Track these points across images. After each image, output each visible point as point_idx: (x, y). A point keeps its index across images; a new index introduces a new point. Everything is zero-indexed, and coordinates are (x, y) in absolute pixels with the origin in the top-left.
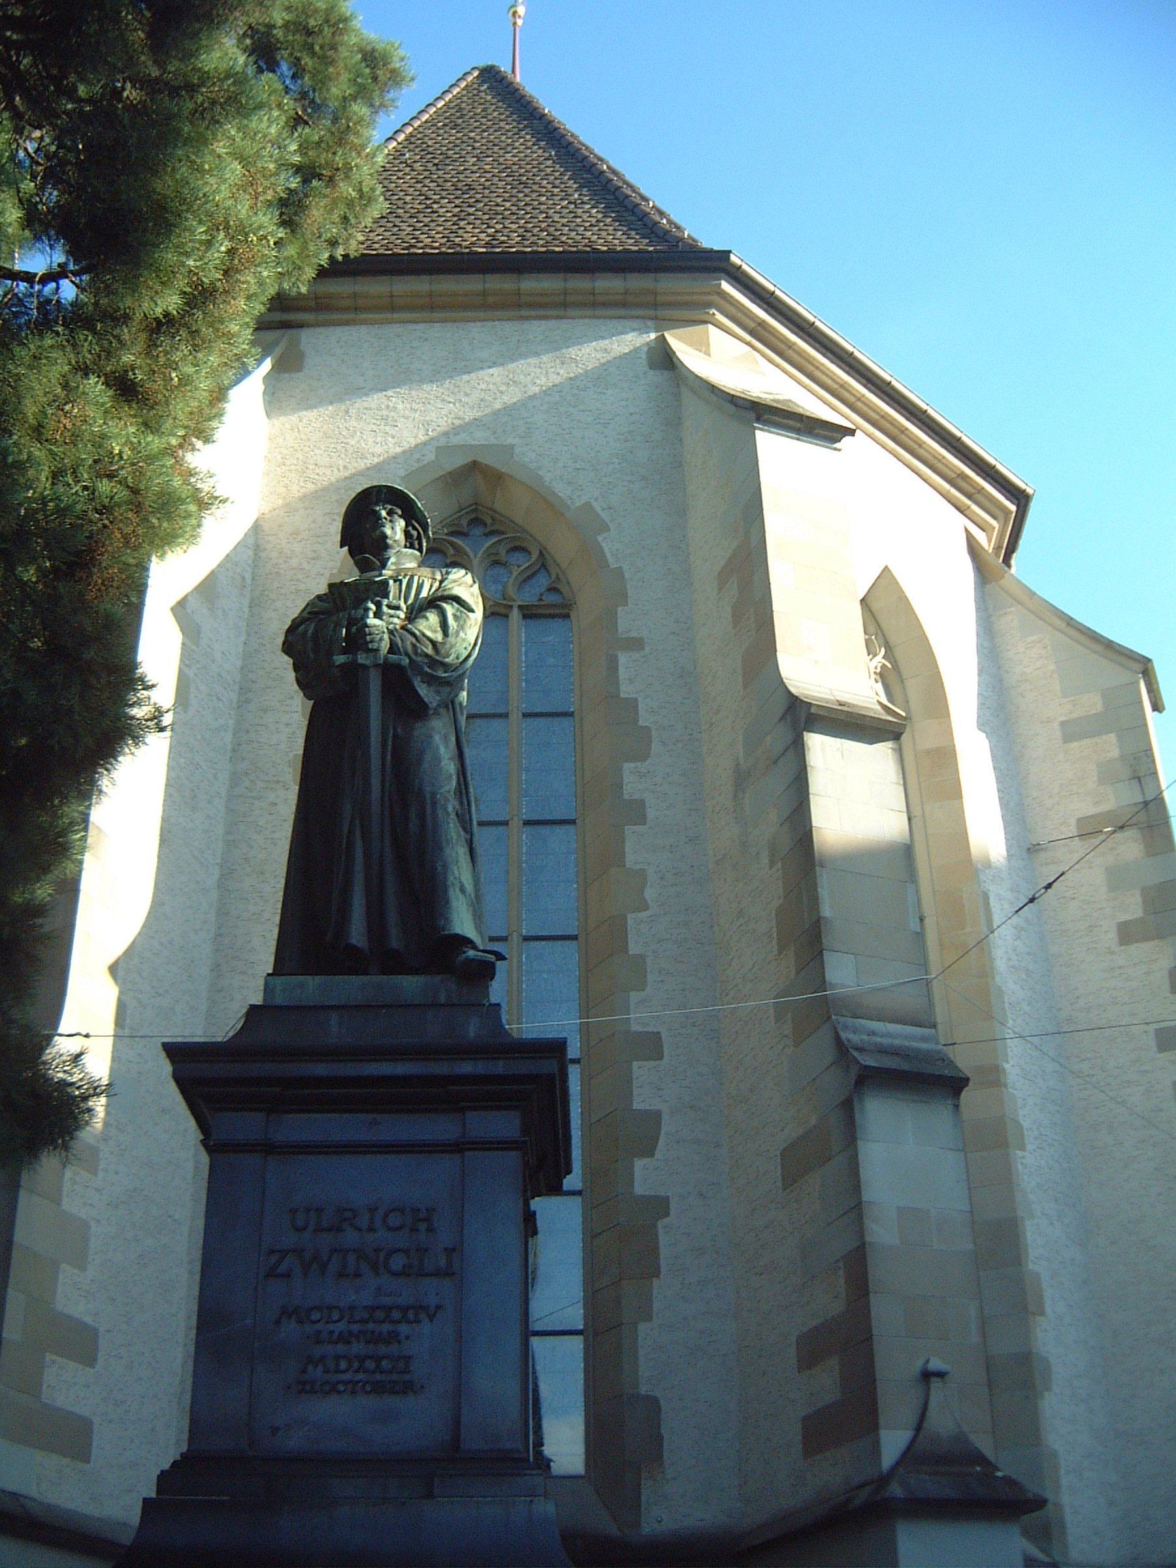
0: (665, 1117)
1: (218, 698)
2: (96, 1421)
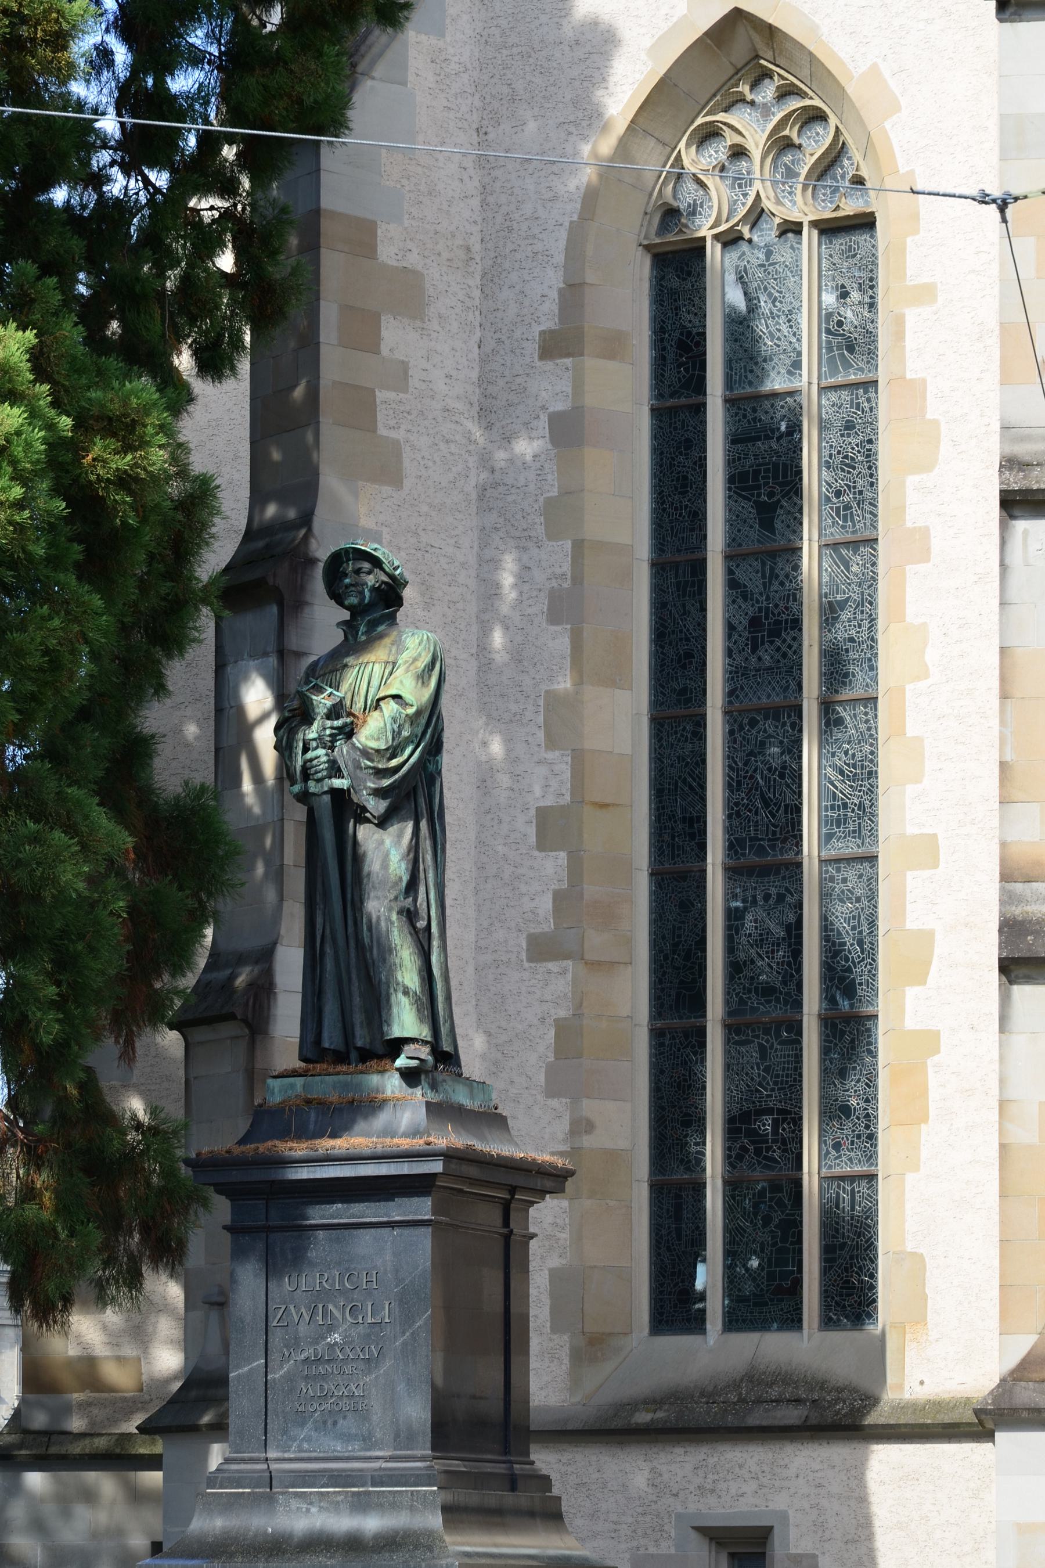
0: (938, 937)
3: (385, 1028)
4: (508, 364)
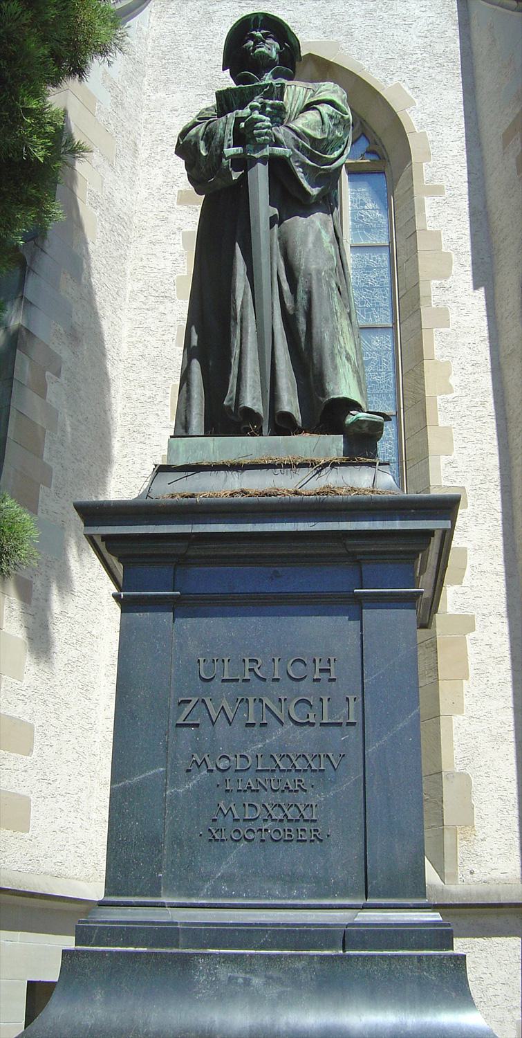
1: (119, 234)
2: (33, 798)
3: (330, 387)
4: (156, 206)
